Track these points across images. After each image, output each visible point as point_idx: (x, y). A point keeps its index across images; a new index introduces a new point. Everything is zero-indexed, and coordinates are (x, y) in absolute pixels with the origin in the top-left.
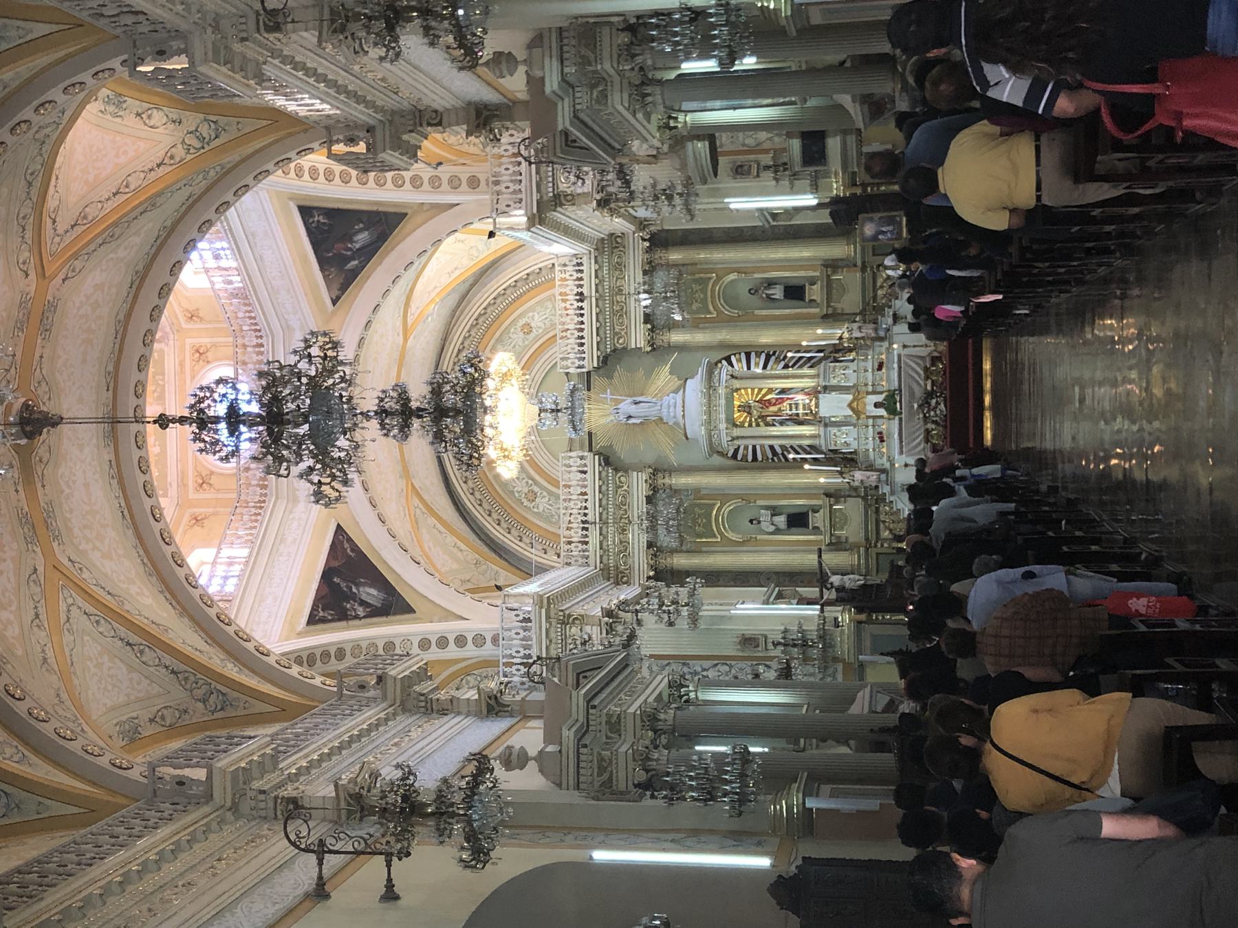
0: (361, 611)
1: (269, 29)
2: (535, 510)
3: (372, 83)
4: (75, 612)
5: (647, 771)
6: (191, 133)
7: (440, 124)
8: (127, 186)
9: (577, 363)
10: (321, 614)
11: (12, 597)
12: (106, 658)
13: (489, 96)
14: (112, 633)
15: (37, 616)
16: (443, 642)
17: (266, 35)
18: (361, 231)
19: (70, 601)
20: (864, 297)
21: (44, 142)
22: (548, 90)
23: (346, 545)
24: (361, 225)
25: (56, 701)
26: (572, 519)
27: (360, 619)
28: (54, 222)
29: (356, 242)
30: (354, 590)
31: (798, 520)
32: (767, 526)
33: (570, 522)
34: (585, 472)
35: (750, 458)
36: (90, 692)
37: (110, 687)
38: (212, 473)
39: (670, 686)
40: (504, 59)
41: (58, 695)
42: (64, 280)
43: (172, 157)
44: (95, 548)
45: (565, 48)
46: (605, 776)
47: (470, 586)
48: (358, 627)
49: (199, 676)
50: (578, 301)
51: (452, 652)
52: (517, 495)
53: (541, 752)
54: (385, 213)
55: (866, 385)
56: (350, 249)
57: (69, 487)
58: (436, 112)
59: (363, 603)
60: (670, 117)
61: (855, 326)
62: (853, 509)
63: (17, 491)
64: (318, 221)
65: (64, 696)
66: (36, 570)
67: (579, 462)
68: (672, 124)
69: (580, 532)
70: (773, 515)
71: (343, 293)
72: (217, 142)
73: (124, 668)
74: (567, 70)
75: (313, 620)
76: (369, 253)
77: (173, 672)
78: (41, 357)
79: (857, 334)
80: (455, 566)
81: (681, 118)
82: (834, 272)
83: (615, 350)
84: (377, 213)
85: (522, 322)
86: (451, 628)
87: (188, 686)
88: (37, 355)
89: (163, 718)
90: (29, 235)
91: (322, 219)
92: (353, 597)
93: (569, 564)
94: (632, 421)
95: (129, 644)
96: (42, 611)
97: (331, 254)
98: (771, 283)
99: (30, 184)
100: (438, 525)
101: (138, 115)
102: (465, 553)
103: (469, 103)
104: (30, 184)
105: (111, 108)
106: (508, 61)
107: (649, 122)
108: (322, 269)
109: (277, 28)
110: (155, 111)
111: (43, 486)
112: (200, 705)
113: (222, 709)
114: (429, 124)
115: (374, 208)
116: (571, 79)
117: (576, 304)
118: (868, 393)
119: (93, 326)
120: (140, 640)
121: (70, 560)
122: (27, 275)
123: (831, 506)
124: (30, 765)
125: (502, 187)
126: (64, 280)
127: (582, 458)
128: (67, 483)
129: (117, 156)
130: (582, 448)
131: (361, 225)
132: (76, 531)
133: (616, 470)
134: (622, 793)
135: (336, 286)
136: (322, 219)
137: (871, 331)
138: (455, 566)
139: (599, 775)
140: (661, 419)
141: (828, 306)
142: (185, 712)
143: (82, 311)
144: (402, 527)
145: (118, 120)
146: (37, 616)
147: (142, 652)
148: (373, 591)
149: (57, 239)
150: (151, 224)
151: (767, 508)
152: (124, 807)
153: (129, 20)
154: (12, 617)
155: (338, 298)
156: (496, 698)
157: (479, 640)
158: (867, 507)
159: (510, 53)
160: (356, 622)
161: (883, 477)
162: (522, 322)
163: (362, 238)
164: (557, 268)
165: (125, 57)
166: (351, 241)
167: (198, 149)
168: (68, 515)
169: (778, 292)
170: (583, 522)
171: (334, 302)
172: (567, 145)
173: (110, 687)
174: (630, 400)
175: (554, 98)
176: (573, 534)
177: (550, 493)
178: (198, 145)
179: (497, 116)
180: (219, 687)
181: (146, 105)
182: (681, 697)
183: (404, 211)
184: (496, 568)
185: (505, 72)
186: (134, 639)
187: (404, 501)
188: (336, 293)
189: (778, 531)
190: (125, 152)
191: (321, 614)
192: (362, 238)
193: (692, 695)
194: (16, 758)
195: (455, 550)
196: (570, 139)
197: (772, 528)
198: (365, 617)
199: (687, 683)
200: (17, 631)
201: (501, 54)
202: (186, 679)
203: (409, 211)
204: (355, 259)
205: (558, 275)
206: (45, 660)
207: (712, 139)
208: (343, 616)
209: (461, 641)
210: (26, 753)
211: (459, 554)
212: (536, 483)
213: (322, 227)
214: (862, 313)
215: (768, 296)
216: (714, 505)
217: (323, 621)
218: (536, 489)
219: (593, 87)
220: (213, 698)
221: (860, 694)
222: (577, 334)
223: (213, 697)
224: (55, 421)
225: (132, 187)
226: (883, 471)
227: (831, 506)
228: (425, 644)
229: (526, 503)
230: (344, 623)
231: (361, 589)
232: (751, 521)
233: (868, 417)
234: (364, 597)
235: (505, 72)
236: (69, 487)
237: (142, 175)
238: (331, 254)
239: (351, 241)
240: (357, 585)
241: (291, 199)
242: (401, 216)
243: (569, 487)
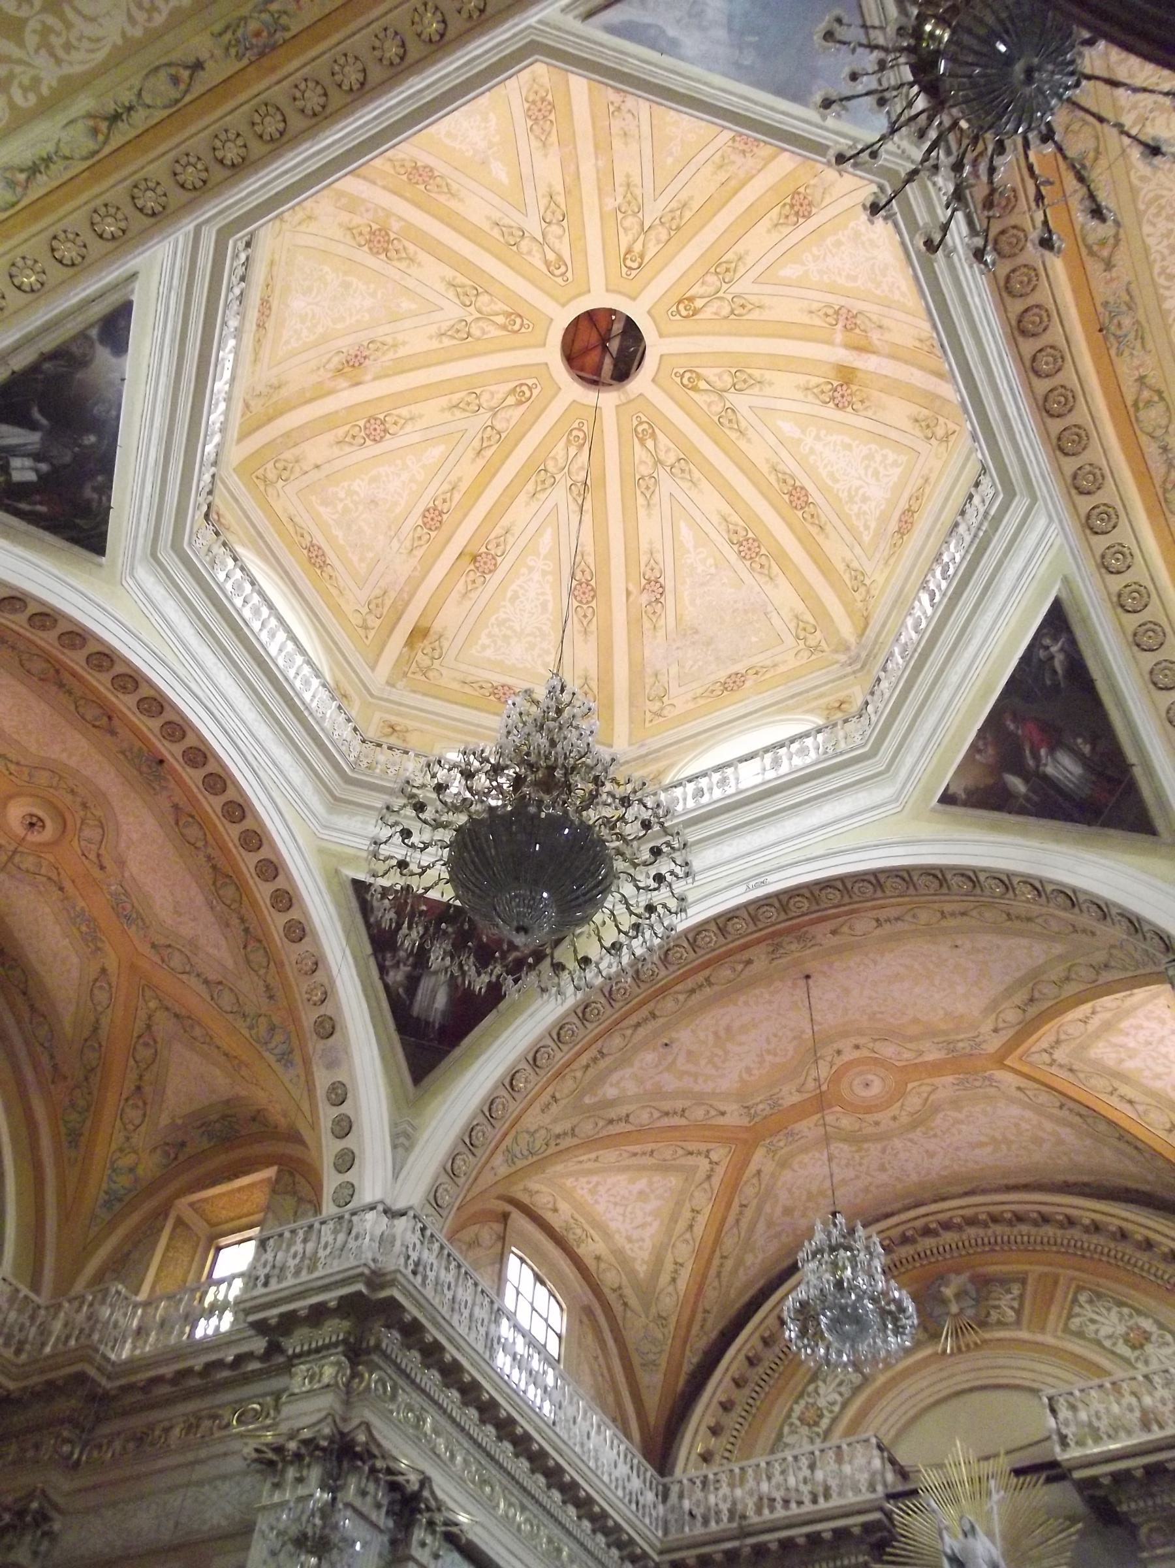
0: (397, 976)
2: (786, 1429)
16: (344, 1128)
24: (1087, 749)
27: (382, 978)
29: (1055, 760)
47: (617, 1308)
51: (330, 1148)
52: (811, 1388)
54: (1131, 788)
56: (1036, 756)
59: (413, 983)
64: (1052, 658)
71: (965, 804)
80: (642, 1269)
85: (1147, 1324)
97: (1012, 727)
100: (702, 1220)
102: (671, 1289)
115: (1131, 756)
131: (1087, 749)
135: (969, 781)
138: (642, 1269)
162: (1147, 1324)
166: (1052, 751)
171: (947, 799)
176: (721, 1493)
184: (664, 1357)
188: (958, 790)
195: (669, 1266)
198: (387, 987)
204: (1026, 780)
211: (665, 1278)
212: (834, 1420)
213: (1047, 675)
217: (366, 909)
218: (825, 1423)
228: (339, 1094)
229: (798, 1409)
230: (368, 949)
238: (1012, 727)
239: (1052, 751)
241: (1066, 580)
243: (812, 1467)
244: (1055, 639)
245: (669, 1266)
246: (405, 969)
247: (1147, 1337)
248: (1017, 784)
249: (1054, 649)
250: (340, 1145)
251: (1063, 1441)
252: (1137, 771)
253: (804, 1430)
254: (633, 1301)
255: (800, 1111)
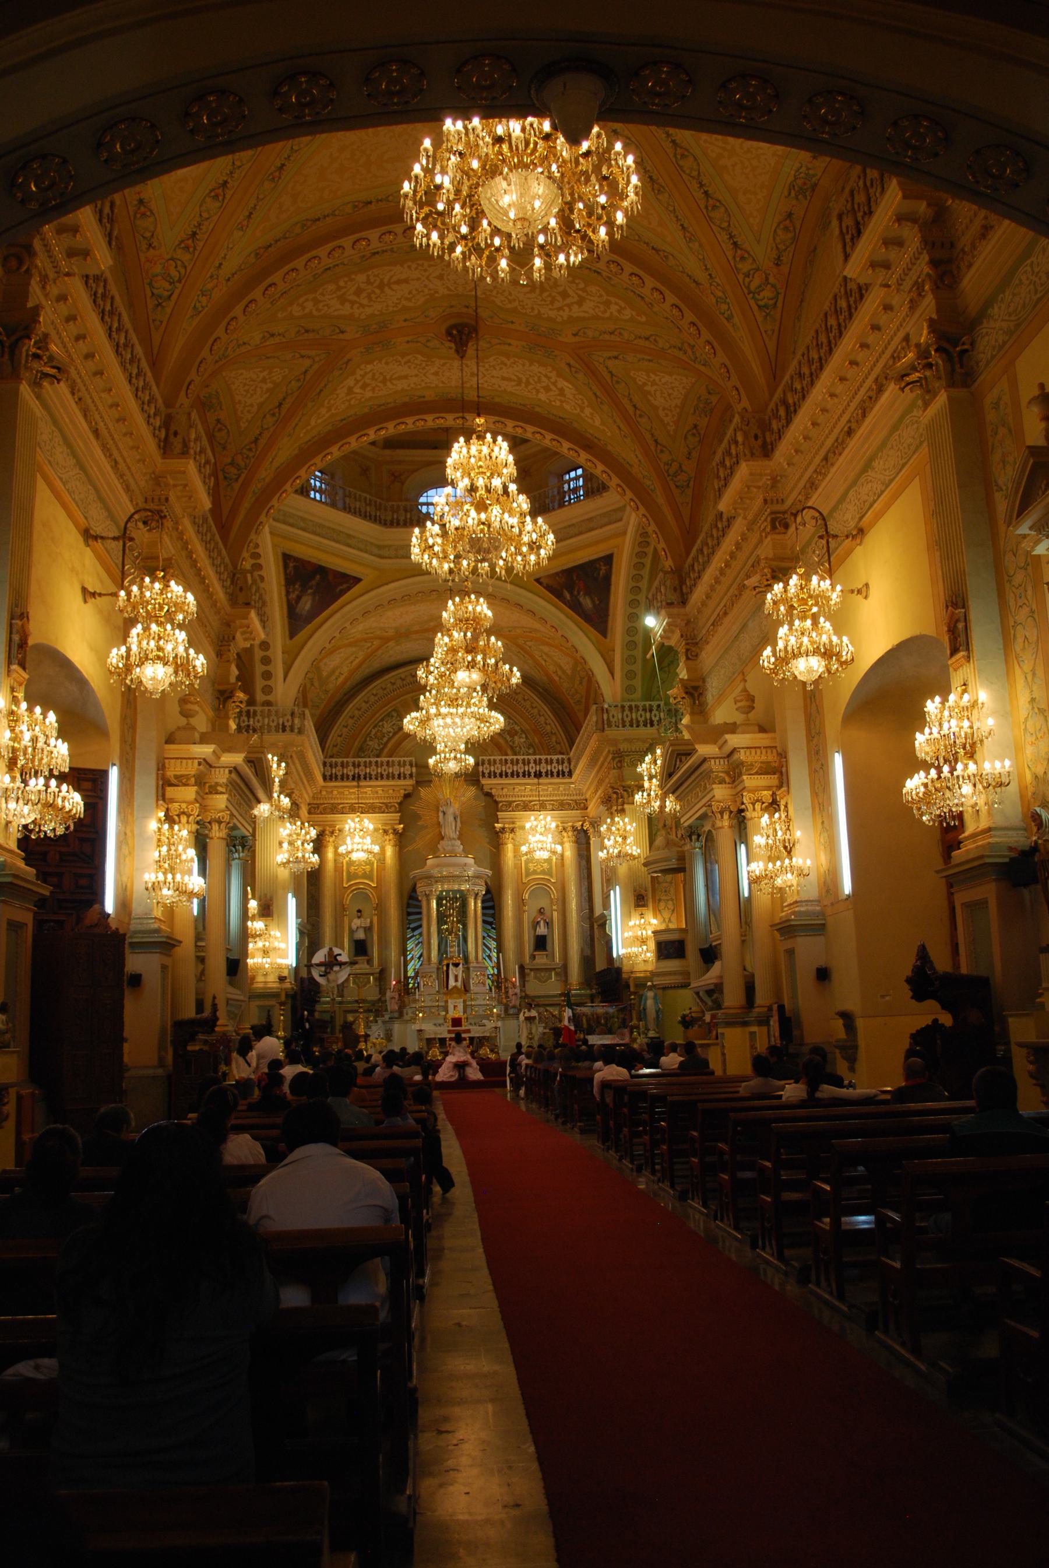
0: (293, 596)
1: (773, 521)
3: (722, 604)
4: (308, 362)
5: (178, 815)
6: (681, 467)
7: (688, 658)
8: (640, 416)
9: (486, 772)
10: (291, 565)
11: (322, 312)
12: (270, 385)
13: (710, 697)
14: (289, 392)
15: (307, 331)
17: (769, 519)
18: (593, 601)
19: (317, 359)
20: (539, 997)
21: (680, 349)
22: (727, 736)
23: (345, 586)
25: (241, 342)
26: (362, 767)
28: (616, 358)
30: (310, 591)
31: (360, 948)
32: (356, 922)
33: (359, 766)
34: (399, 777)
35: (410, 910)
36: (244, 371)
37: (247, 388)
38: (403, 484)
39: (243, 837)
40: (748, 703)
41: (244, 343)
42: (569, 364)
43: (662, 451)
44: (357, 381)
45: (758, 751)
46: (174, 781)
47: (309, 685)
48: (280, 594)
49: (253, 460)
50: (535, 773)
53: (194, 728)
54: (606, 622)
55: (472, 1000)
57: (405, 363)
58: (697, 656)
59: (299, 598)
60: (699, 836)
61: (518, 990)
62: (371, 993)
63: (405, 320)
65: (243, 349)
66: (343, 332)
67: (408, 773)
68: (694, 837)
69: (351, 774)
70: (365, 928)
72: (673, 487)
73: (262, 399)
74: (742, 751)
75: (287, 558)
76: (576, 607)
77: (257, 439)
78: (510, 344)
79: (511, 992)
80: (325, 674)
81: (698, 844)
82: (557, 974)
83: (496, 802)
84: (607, 615)
86: (278, 668)
87: (245, 451)
88: (509, 341)
89: (220, 430)
90: (607, 337)
91: (602, 573)
92: (304, 590)
93: (325, 764)
94: (441, 815)
95: (280, 405)
96: (311, 335)
98: (548, 924)
99: (647, 339)
100: (357, 661)
101: (695, 426)
103: (704, 680)
104: (647, 339)
105: (701, 406)
106: (749, 707)
107: (697, 819)
108: (563, 572)
109: (774, 527)
110: (697, 439)
111: (408, 342)
112: (229, 460)
113: (225, 478)
114: (687, 650)
116: (735, 756)
117: (532, 771)
118: (464, 1002)
119: (530, 387)
120: (283, 414)
121: (349, 360)
122: (575, 335)
123: (372, 974)
124: (192, 316)
125: (627, 712)
126: (569, 364)
127: (411, 776)
128: (409, 361)
129: (664, 409)
130: (418, 774)
132: (369, 367)
133: (400, 804)
134: (164, 795)
136: (602, 573)
137: (513, 1003)
138: (325, 674)
139: (176, 777)
140: (443, 838)
141: (531, 970)
142: (224, 448)
143: (544, 379)
144: (358, 630)
145: (692, 411)
146: (307, 331)
147: (273, 415)
148: (308, 606)
149: (601, 360)
150: (609, 434)
151: (371, 922)
152: (158, 387)
153: (782, 412)
154: (307, 311)
155: (541, 584)
156: (231, 697)
157: (268, 690)
158: (374, 1003)
159: (753, 708)
160: (284, 593)
161: (396, 1015)
163: (587, 602)
164: (560, 757)
165: (749, 409)
166: (585, 594)
167: (667, 471)
168: (384, 361)
169: (542, 930)
170: (359, 776)
172: (678, 755)
173: (247, 388)
174: (458, 813)
175: (721, 742)
177: (382, 749)
178: (671, 472)
179: (694, 703)
180: (243, 476)
181: (702, 432)
182: (234, 846)
183: (609, 635)
185: (739, 704)
186: (286, 406)
187: (378, 632)
188: (544, 581)
189: (352, 932)
190: (667, 415)
191: (291, 565)
192: (587, 602)
193: (236, 855)
194: (198, 305)
195: (337, 673)
196: (683, 758)
197: (354, 927)
198: (288, 601)
199: (246, 851)
200: (296, 314)
201: (753, 701)
202: (250, 450)
203: (608, 640)
205: (555, 757)
206: (273, 335)
207: (682, 870)
208: (289, 581)
209: (267, 675)
210: (201, 315)
211: (334, 677)
212: (389, 740)
214: (527, 996)
215: (538, 923)
216: (372, 881)
217: (286, 566)
219: (727, 773)
220: (233, 470)
221: (238, 992)
222: (509, 771)
223: (236, 472)
224: (461, 353)
225: (639, 420)
226: (401, 1014)
227: (372, 974)
229: (374, 732)
230: (283, 582)
231: (310, 597)
232: (359, 911)
233: (447, 1002)
234: (304, 599)
235: (739, 704)
236: (405, 363)
237: (649, 428)
240: (314, 594)
242: (604, 632)
244: (605, 565)
245: (337, 673)
246: (297, 593)
247: (516, 733)
248: (568, 596)
249: (603, 568)
250: (265, 668)
251: (483, 774)
252: (610, 618)
253: (376, 740)
254: (316, 684)
255: (417, 632)
